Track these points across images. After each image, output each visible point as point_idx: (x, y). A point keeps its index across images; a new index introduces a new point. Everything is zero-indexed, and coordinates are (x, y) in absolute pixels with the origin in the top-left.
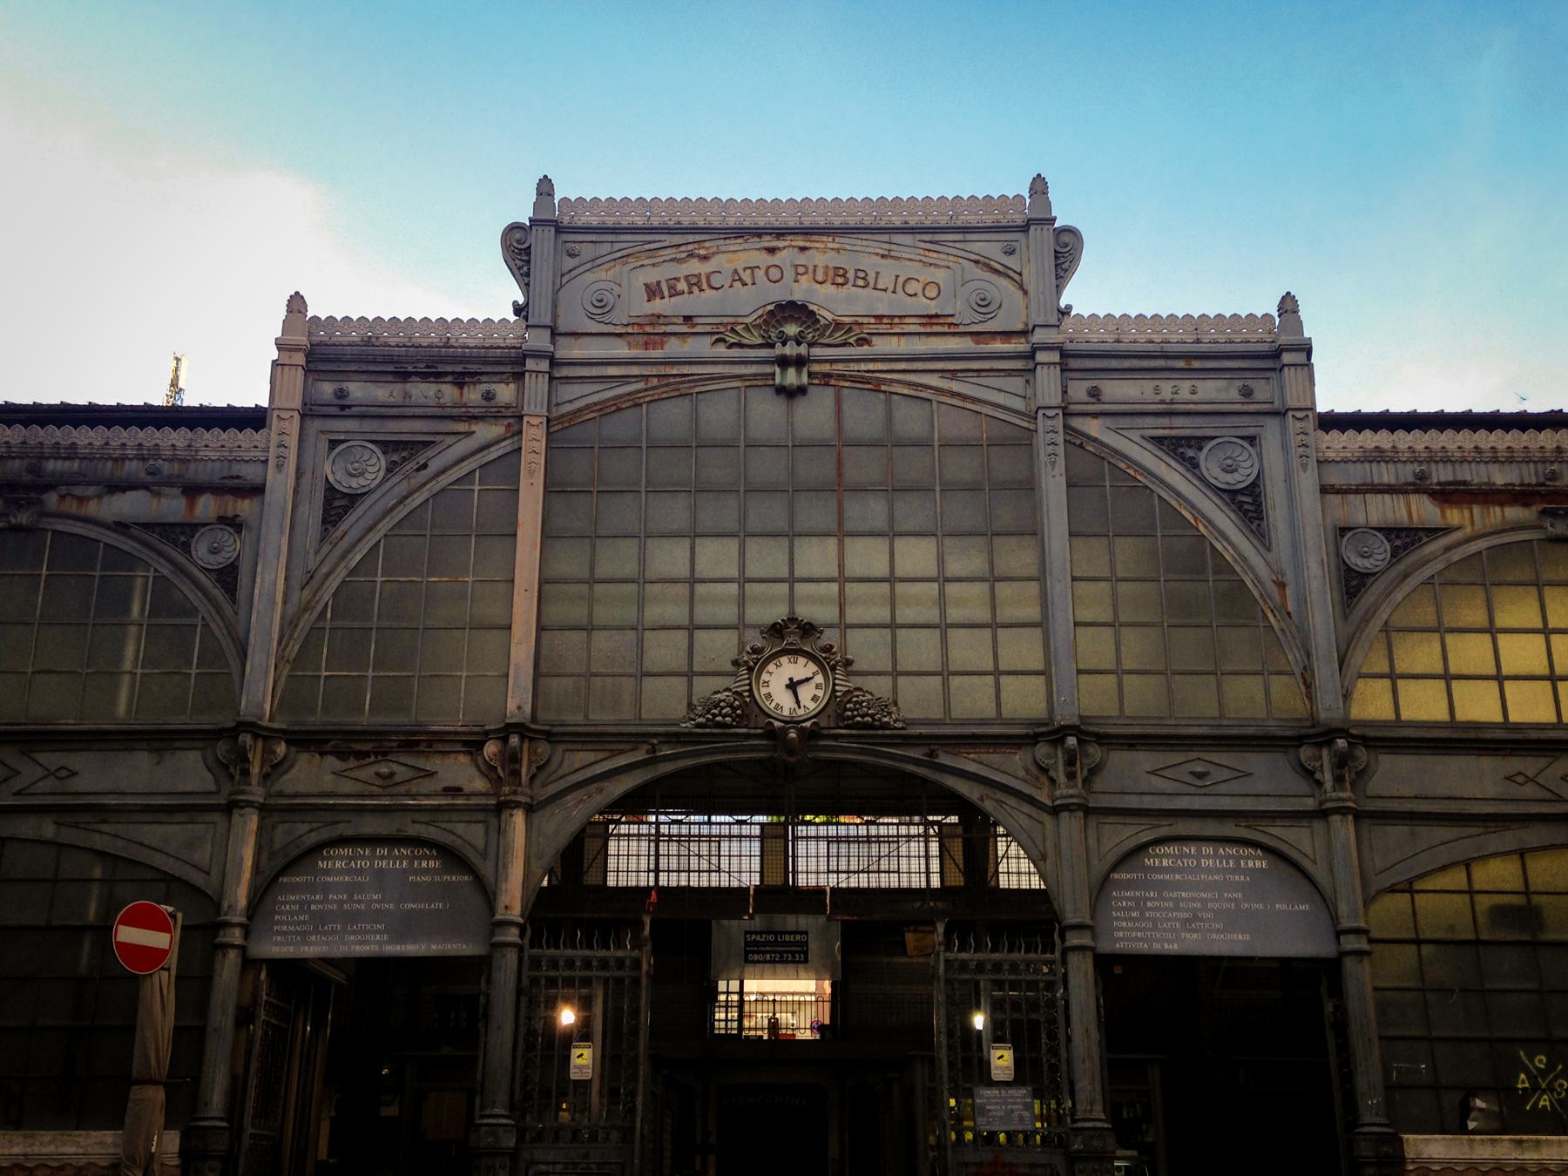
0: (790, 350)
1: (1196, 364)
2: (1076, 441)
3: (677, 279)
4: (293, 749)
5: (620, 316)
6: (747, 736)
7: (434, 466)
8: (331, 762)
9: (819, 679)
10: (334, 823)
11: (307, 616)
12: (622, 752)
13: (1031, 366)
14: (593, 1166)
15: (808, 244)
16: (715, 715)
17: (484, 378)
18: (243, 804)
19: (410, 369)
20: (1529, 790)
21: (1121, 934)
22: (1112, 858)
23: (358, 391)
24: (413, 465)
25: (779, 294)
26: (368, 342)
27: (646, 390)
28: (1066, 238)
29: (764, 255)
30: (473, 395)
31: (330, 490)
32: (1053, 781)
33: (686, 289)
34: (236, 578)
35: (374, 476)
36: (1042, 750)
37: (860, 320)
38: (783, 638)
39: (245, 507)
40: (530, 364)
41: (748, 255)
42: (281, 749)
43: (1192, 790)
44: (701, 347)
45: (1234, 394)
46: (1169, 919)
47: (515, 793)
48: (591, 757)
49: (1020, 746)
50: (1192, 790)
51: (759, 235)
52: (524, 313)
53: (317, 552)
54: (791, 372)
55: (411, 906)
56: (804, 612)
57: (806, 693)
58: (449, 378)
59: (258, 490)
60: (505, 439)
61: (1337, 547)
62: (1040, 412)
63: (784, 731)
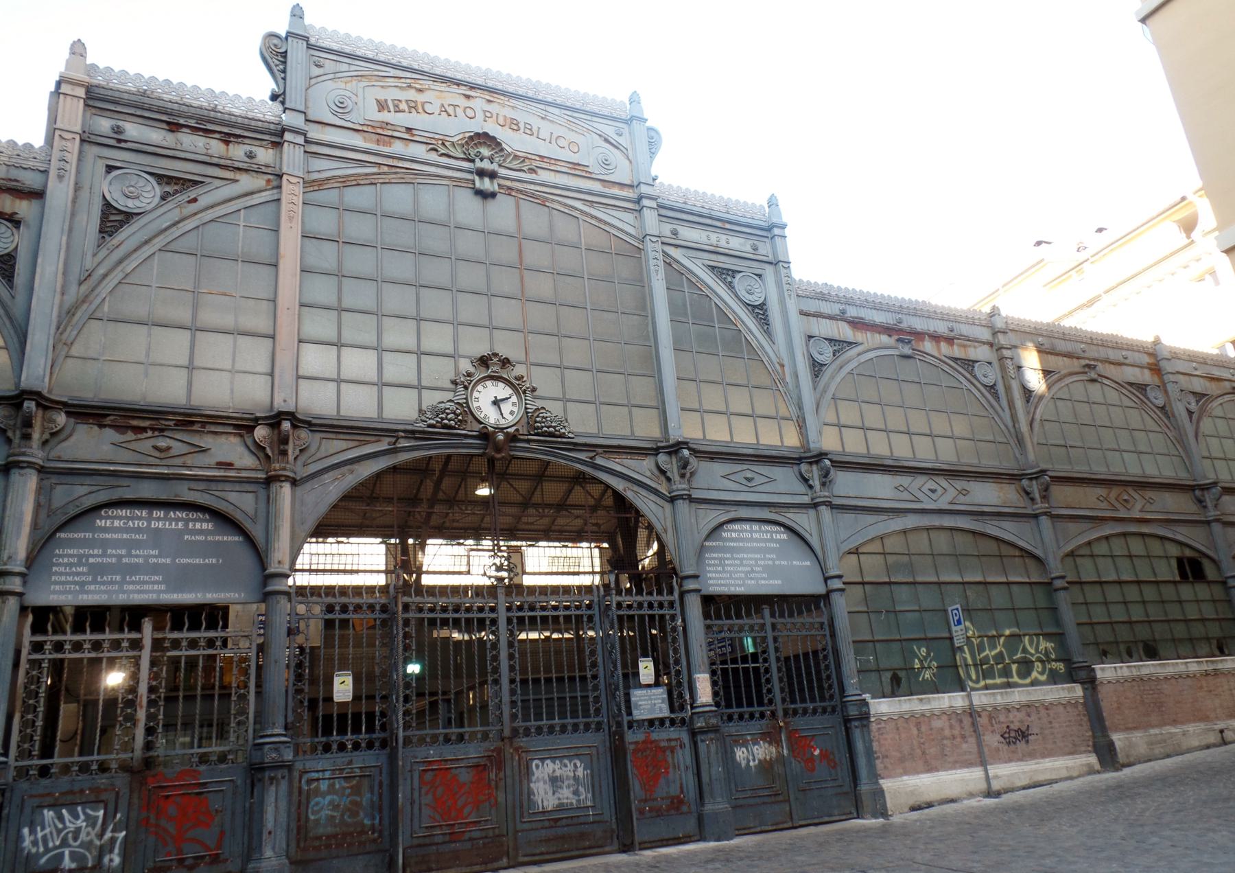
0: (485, 165)
1: (728, 226)
2: (669, 262)
3: (400, 101)
4: (72, 420)
5: (356, 118)
6: (466, 436)
7: (204, 201)
8: (110, 434)
9: (514, 399)
10: (114, 487)
11: (85, 306)
12: (368, 442)
13: (637, 207)
14: (357, 770)
15: (492, 99)
16: (442, 419)
17: (247, 141)
18: (25, 465)
19: (182, 121)
20: (905, 495)
21: (712, 582)
22: (705, 532)
23: (133, 130)
24: (183, 197)
25: (477, 126)
26: (144, 94)
27: (379, 174)
28: (653, 134)
29: (463, 98)
30: (238, 152)
31: (108, 207)
32: (669, 479)
33: (407, 110)
34: (13, 266)
35: (148, 201)
36: (662, 458)
37: (530, 156)
38: (488, 367)
39: (23, 208)
40: (288, 136)
41: (453, 96)
42: (61, 419)
43: (746, 489)
44: (419, 151)
45: (748, 248)
46: (739, 572)
47: (284, 469)
48: (343, 445)
49: (646, 455)
50: (746, 489)
51: (458, 85)
52: (280, 99)
53: (94, 255)
54: (487, 180)
55: (185, 561)
56: (504, 352)
57: (506, 408)
58: (217, 136)
59: (38, 195)
60: (266, 190)
61: (807, 345)
62: (648, 237)
63: (495, 433)
